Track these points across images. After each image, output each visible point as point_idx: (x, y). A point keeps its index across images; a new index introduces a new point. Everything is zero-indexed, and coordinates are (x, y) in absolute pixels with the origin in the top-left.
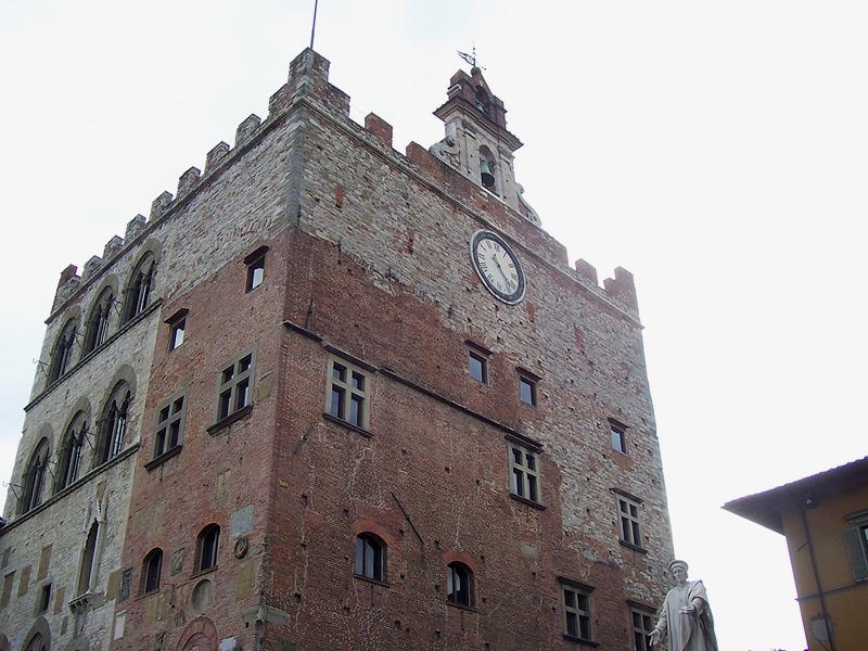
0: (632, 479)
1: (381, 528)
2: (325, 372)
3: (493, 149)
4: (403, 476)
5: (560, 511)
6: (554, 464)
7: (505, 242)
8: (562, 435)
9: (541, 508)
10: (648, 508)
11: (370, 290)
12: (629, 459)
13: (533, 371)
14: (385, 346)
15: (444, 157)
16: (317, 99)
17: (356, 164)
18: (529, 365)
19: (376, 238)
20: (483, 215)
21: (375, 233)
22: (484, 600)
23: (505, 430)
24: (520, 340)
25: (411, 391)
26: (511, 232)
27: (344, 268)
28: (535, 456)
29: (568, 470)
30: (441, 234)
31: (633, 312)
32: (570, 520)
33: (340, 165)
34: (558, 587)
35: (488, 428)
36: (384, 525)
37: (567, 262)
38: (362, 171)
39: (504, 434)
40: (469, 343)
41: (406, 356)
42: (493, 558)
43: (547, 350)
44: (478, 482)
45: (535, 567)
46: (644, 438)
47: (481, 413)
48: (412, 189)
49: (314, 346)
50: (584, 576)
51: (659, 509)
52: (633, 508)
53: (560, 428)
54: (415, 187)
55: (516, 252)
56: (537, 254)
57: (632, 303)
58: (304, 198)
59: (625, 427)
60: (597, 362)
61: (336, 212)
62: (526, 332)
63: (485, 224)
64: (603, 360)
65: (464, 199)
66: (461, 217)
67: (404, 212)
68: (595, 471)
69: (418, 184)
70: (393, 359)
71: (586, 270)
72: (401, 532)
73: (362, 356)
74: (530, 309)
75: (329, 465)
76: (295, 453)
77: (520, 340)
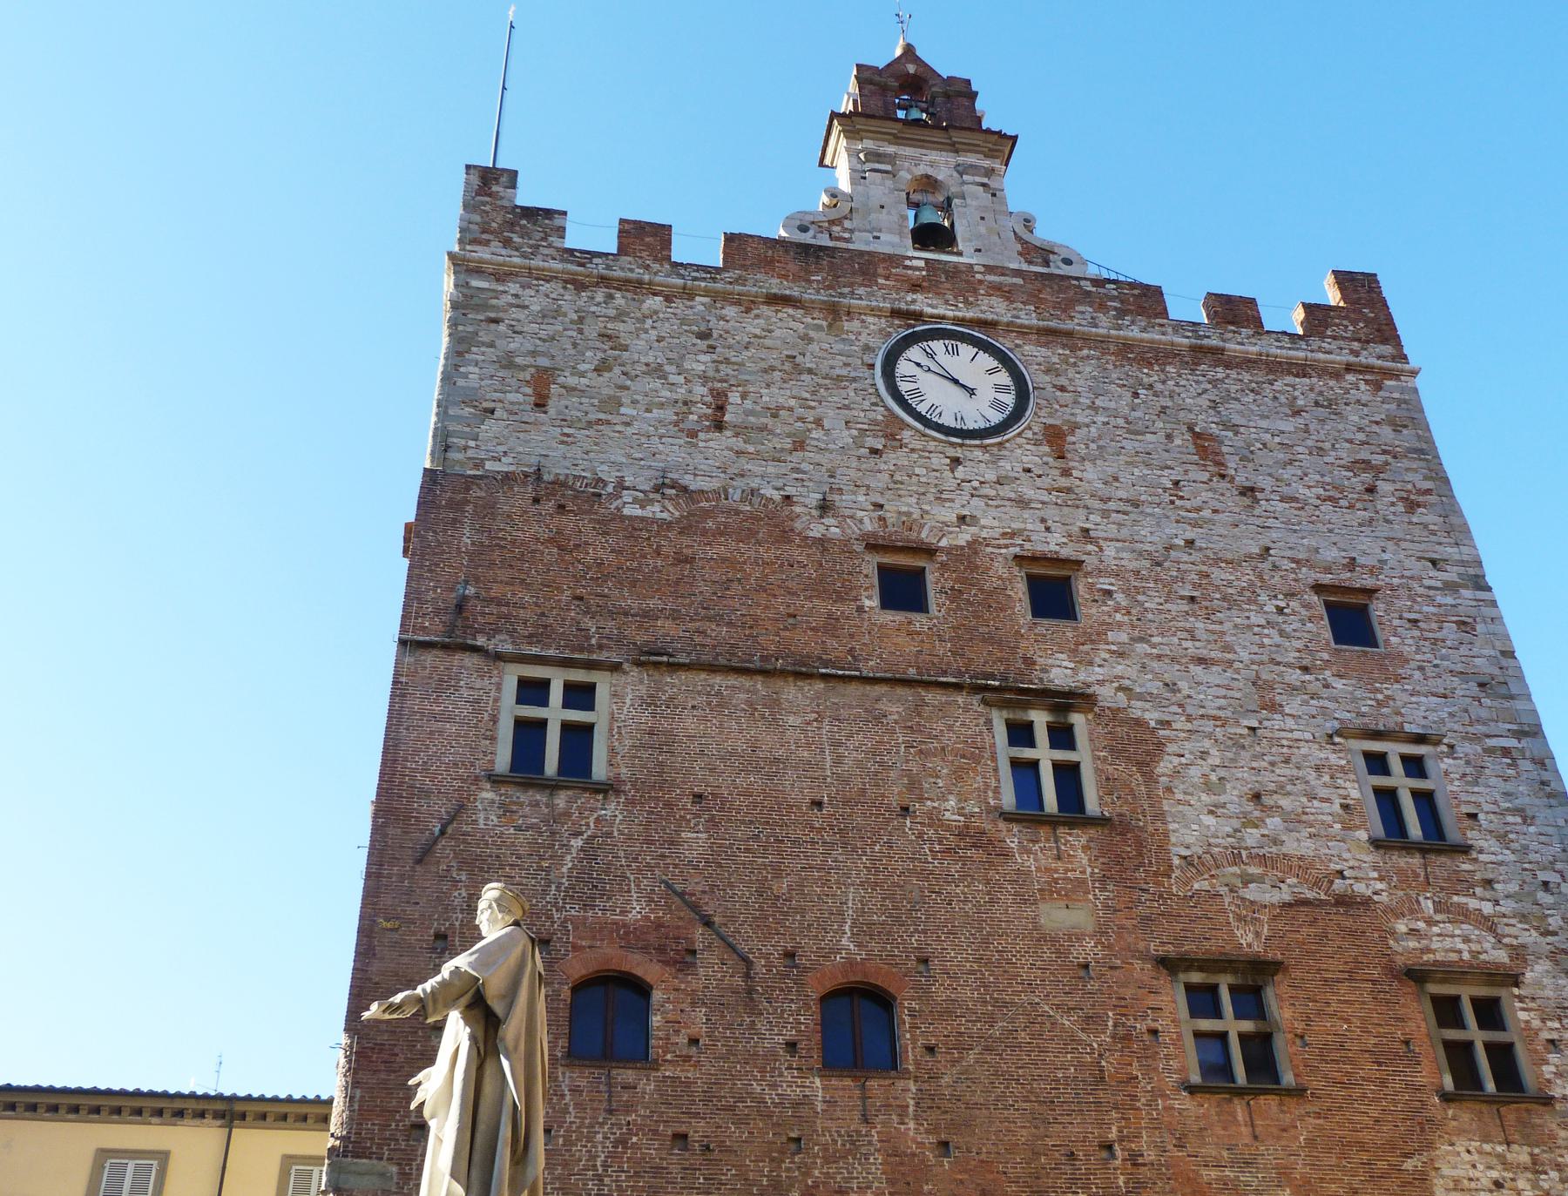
0: (1402, 698)
1: (637, 957)
2: (496, 700)
3: (941, 175)
4: (695, 841)
5: (1160, 816)
6: (1139, 723)
7: (980, 335)
8: (1159, 657)
9: (1101, 822)
10: (1464, 748)
11: (612, 526)
12: (1400, 654)
13: (1065, 553)
14: (646, 614)
15: (811, 233)
16: (487, 243)
17: (581, 320)
18: (1054, 543)
19: (630, 430)
20: (914, 301)
21: (627, 424)
22: (930, 1050)
23: (977, 689)
24: (1022, 503)
25: (717, 680)
26: (997, 309)
27: (549, 506)
28: (1078, 720)
29: (1189, 726)
30: (798, 370)
31: (1387, 349)
32: (1193, 827)
33: (543, 334)
34: (1163, 980)
35: (933, 697)
36: (645, 949)
37: (1164, 313)
38: (591, 330)
39: (975, 700)
40: (872, 547)
41: (709, 619)
42: (956, 954)
43: (1110, 499)
44: (905, 809)
45: (1088, 950)
46: (1449, 600)
47: (912, 672)
48: (722, 318)
49: (470, 660)
50: (1248, 940)
51: (1511, 743)
52: (1405, 759)
53: (1154, 646)
54: (730, 311)
55: (1004, 344)
56: (1069, 325)
57: (1385, 331)
58: (458, 419)
59: (1370, 592)
60: (1264, 482)
61: (531, 417)
62: (1046, 482)
63: (918, 316)
64: (1287, 474)
65: (861, 291)
66: (856, 324)
67: (700, 363)
68: (1274, 707)
69: (738, 303)
70: (666, 628)
71: (1233, 311)
72: (694, 952)
73: (590, 650)
74: (1055, 438)
75: (502, 867)
76: (419, 861)
77: (1022, 503)
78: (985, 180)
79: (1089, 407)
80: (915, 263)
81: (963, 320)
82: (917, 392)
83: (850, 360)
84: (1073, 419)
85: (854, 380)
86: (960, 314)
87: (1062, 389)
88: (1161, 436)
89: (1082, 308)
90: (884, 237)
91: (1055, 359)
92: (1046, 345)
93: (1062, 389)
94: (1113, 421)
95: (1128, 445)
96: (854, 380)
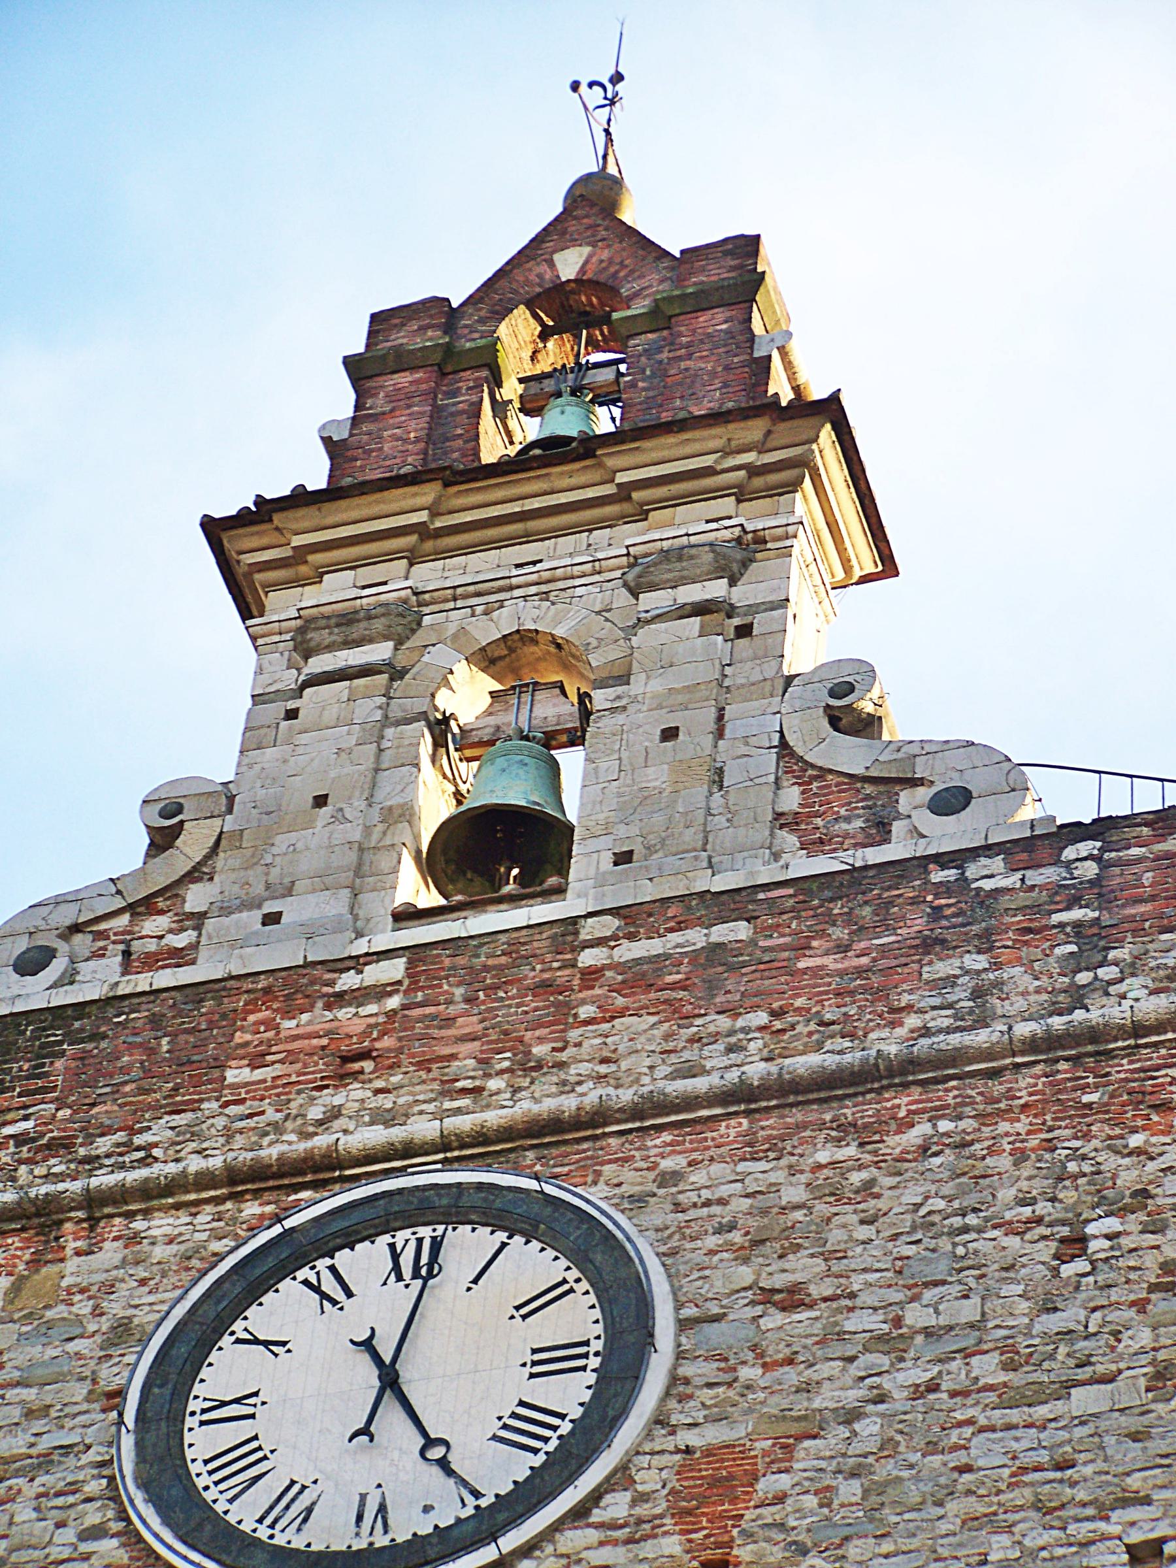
65: (159, 1132)
78: (717, 589)
79: (878, 1342)
80: (376, 973)
81: (481, 1137)
82: (248, 1459)
83: (49, 1395)
84: (801, 1404)
85: (45, 1462)
86: (493, 1118)
87: (792, 1299)
88: (1132, 1388)
89: (942, 968)
90: (293, 910)
91: (794, 1193)
92: (775, 1148)
93: (792, 1299)
94: (956, 1373)
95: (987, 1453)
96: (45, 1462)
